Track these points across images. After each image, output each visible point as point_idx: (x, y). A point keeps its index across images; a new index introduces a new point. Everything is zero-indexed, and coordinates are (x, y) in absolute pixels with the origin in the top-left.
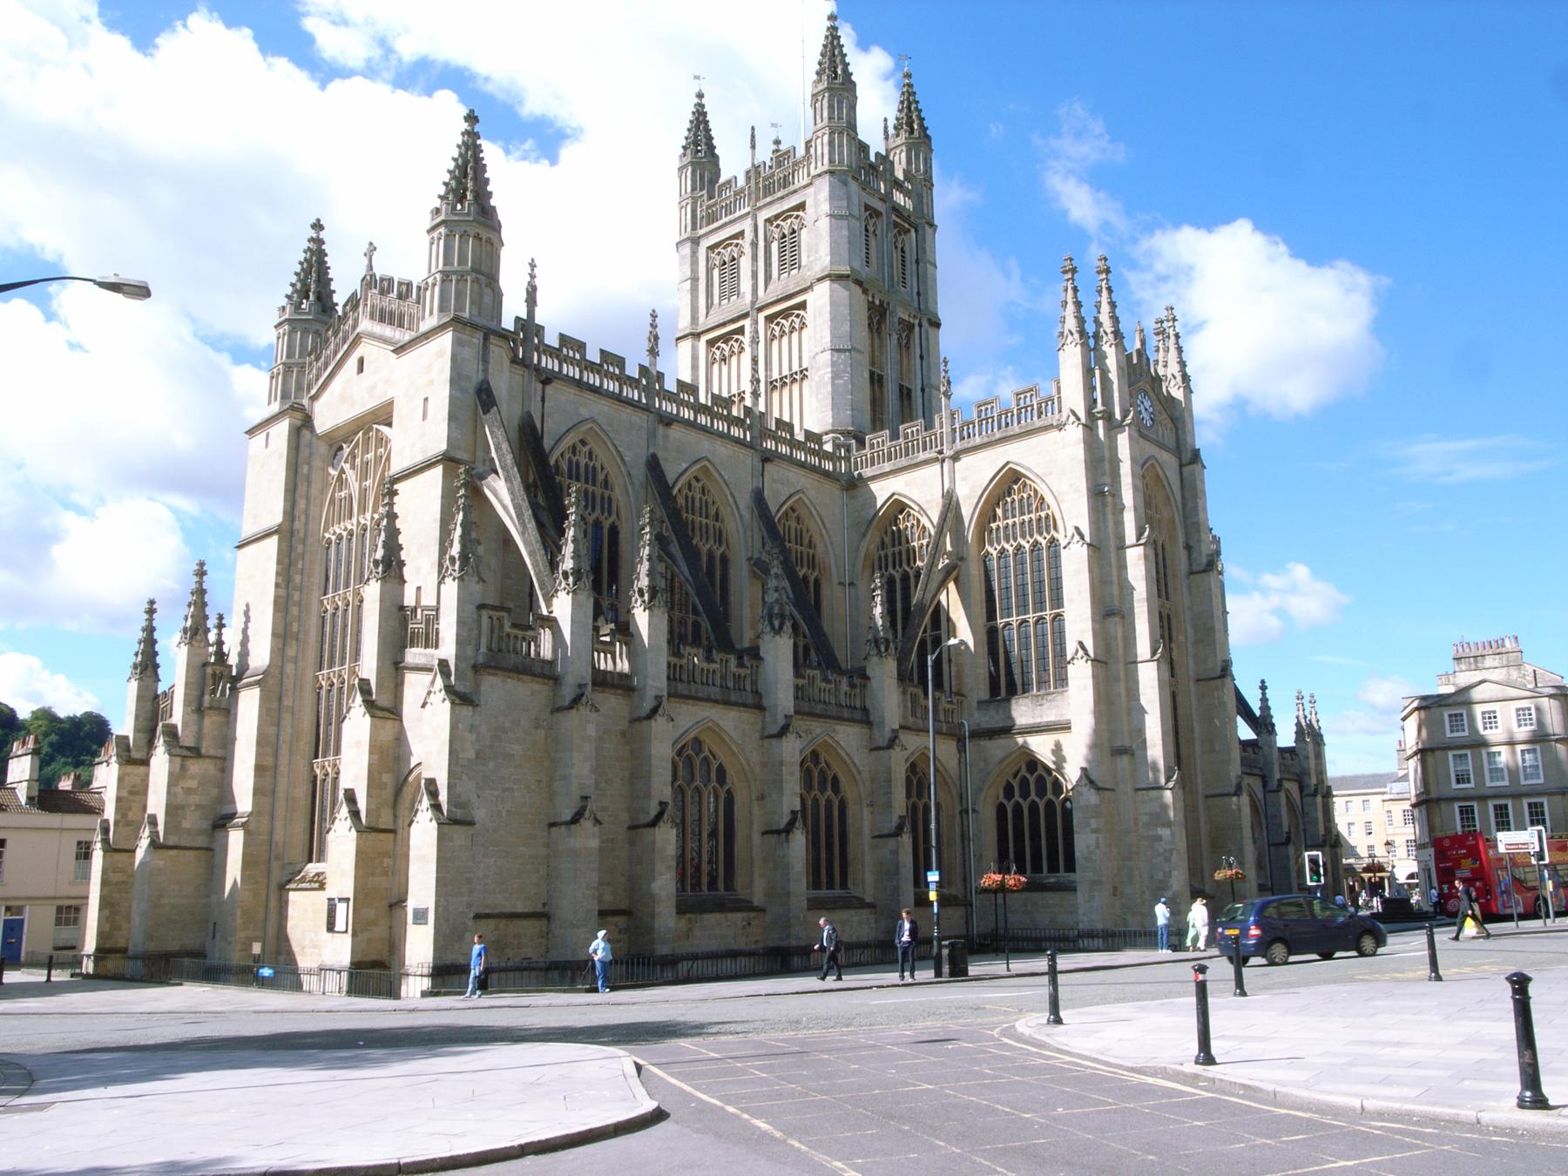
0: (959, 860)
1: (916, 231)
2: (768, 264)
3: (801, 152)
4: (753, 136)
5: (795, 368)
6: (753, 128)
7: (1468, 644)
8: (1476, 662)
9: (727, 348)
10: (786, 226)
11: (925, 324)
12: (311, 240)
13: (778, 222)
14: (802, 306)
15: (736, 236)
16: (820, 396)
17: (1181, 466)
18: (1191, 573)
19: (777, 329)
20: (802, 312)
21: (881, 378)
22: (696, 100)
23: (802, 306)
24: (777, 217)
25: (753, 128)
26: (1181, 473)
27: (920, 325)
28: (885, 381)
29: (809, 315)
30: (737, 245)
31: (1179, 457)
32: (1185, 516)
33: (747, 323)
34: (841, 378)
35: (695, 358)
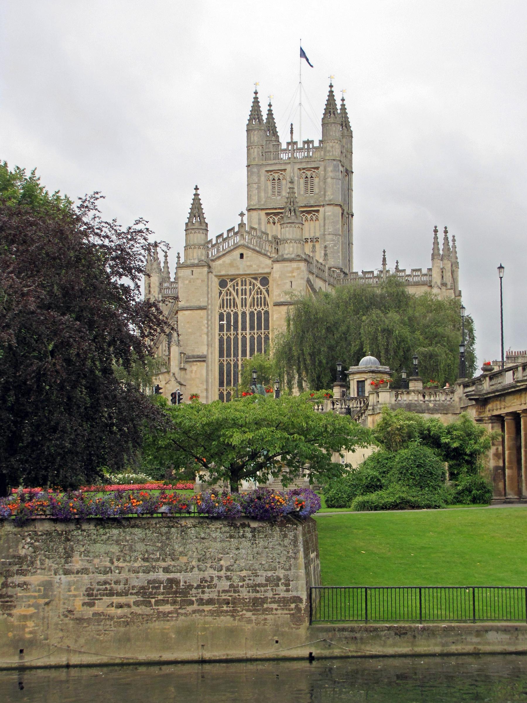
2: (299, 188)
3: (316, 144)
4: (292, 128)
5: (312, 235)
6: (292, 125)
7: (512, 352)
8: (515, 360)
9: (276, 219)
10: (309, 173)
11: (350, 216)
12: (195, 195)
13: (304, 171)
14: (318, 211)
15: (281, 170)
19: (304, 218)
20: (316, 214)
22: (254, 95)
24: (304, 169)
25: (292, 125)
29: (321, 215)
30: (282, 174)
34: (336, 246)
35: (260, 219)
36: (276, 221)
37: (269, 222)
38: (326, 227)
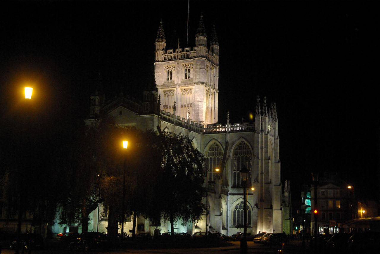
0: (226, 221)
1: (215, 69)
14: (191, 89)
16: (196, 113)
17: (275, 139)
18: (275, 163)
21: (207, 107)
23: (191, 89)
26: (275, 141)
27: (215, 93)
28: (208, 108)
31: (275, 137)
32: (275, 150)
33: (175, 89)
36: (169, 95)
37: (165, 96)
38: (196, 98)
